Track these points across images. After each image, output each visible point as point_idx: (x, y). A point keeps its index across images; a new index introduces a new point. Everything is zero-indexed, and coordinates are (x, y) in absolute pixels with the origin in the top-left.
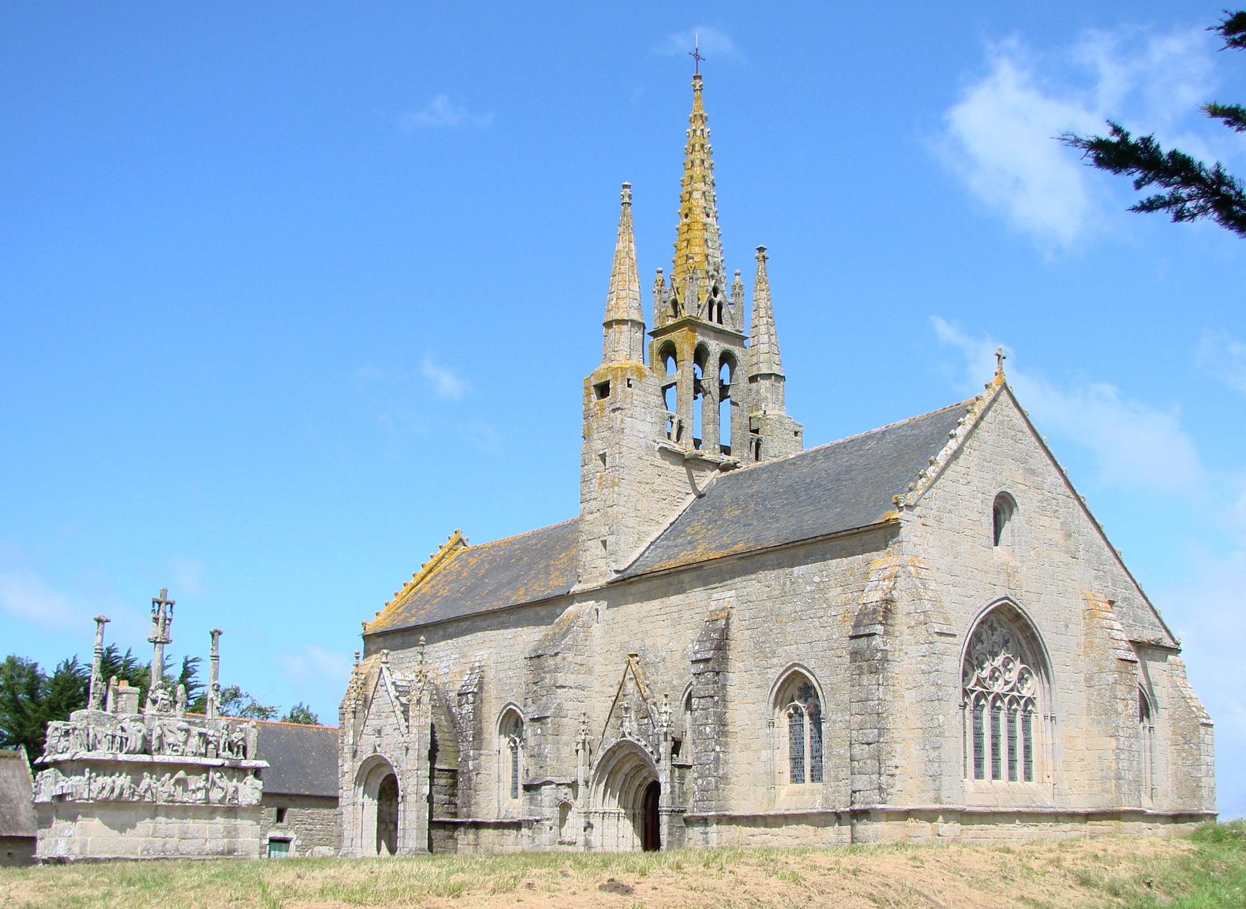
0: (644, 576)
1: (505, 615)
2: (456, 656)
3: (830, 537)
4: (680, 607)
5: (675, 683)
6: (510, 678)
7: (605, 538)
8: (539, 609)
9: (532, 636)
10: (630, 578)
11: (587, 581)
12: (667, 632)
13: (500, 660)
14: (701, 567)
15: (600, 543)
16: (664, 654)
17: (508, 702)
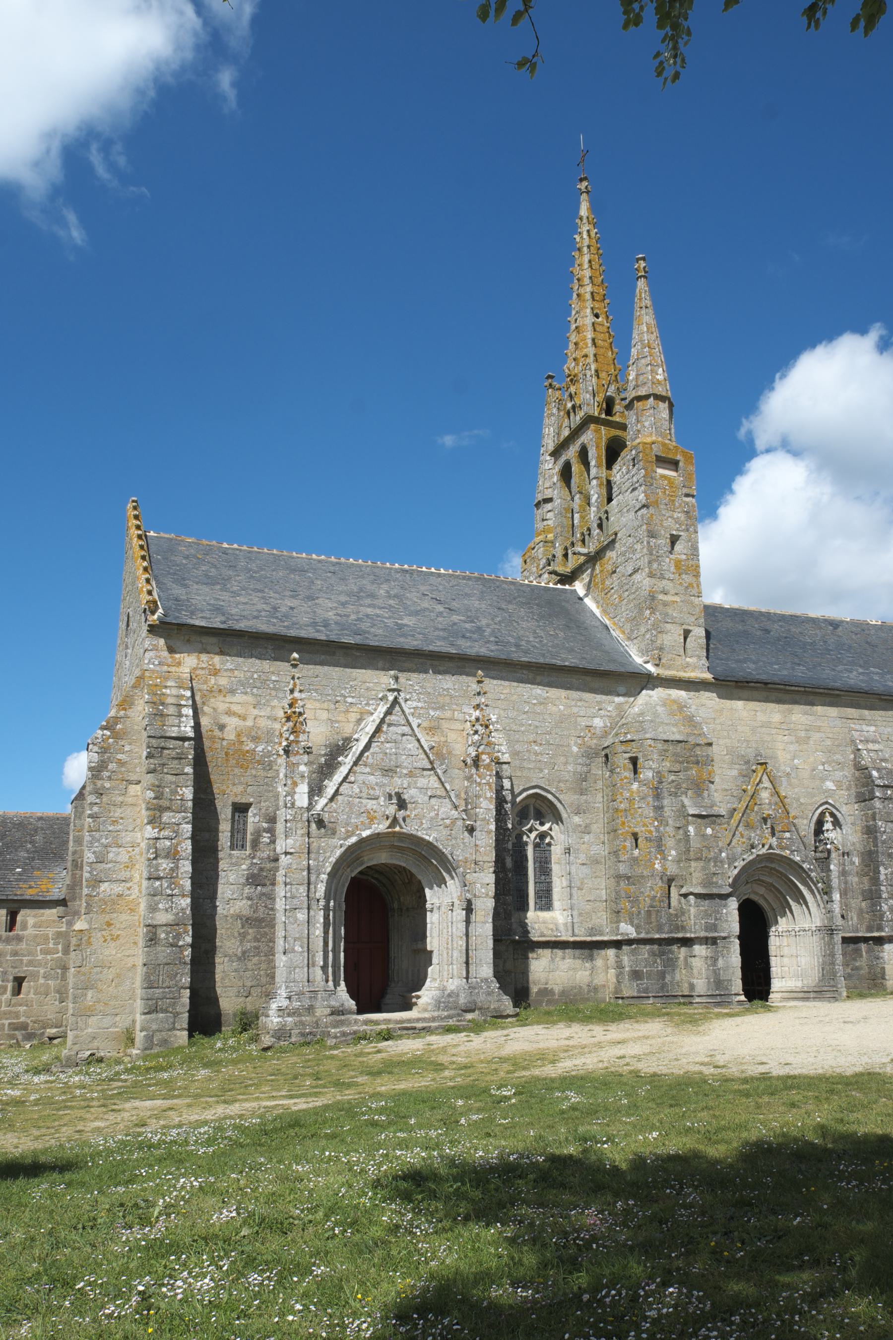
0: (770, 686)
1: (524, 672)
2: (420, 705)
3: (832, 692)
4: (808, 728)
5: (802, 800)
6: (536, 754)
7: (690, 628)
8: (588, 679)
9: (575, 710)
10: (748, 682)
11: (669, 668)
12: (792, 748)
13: (514, 728)
14: (838, 695)
15: (682, 632)
16: (788, 770)
17: (533, 784)
